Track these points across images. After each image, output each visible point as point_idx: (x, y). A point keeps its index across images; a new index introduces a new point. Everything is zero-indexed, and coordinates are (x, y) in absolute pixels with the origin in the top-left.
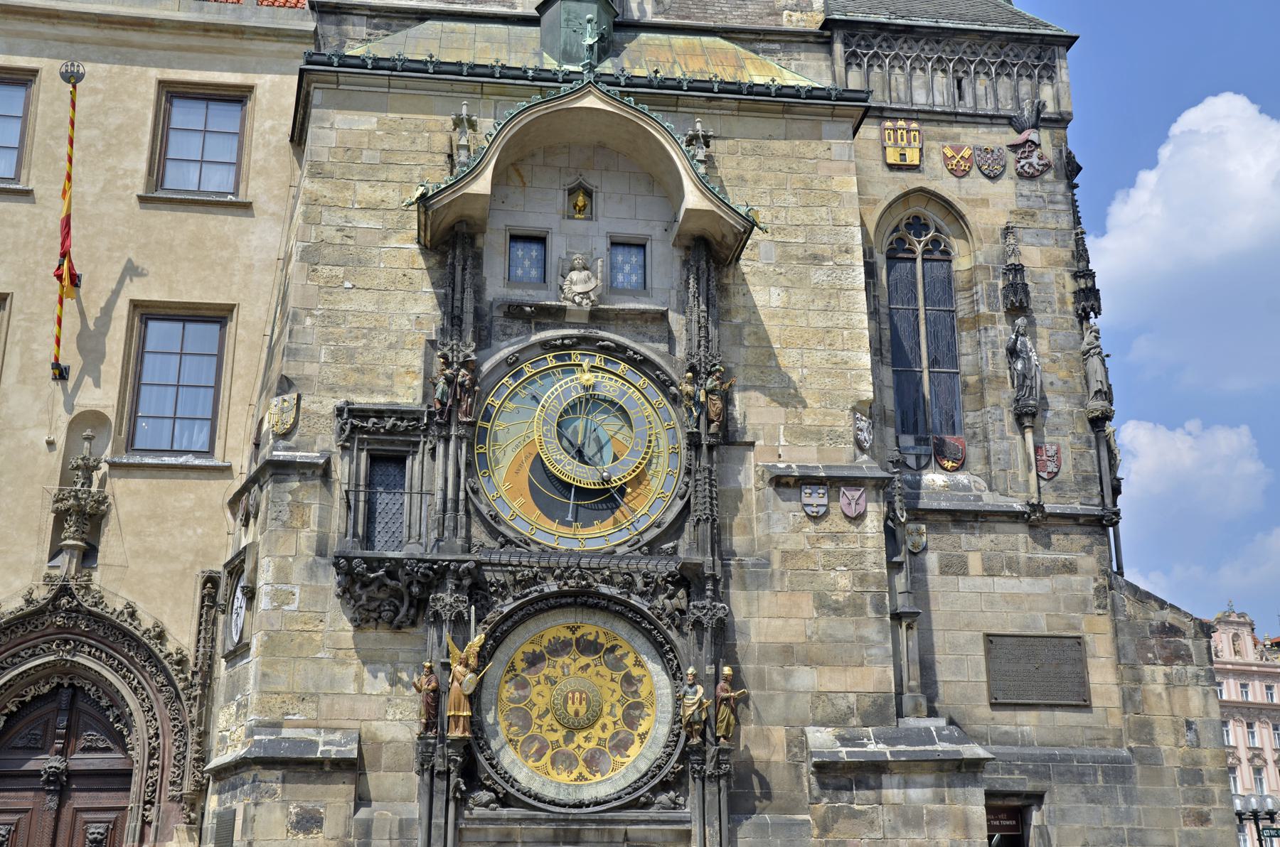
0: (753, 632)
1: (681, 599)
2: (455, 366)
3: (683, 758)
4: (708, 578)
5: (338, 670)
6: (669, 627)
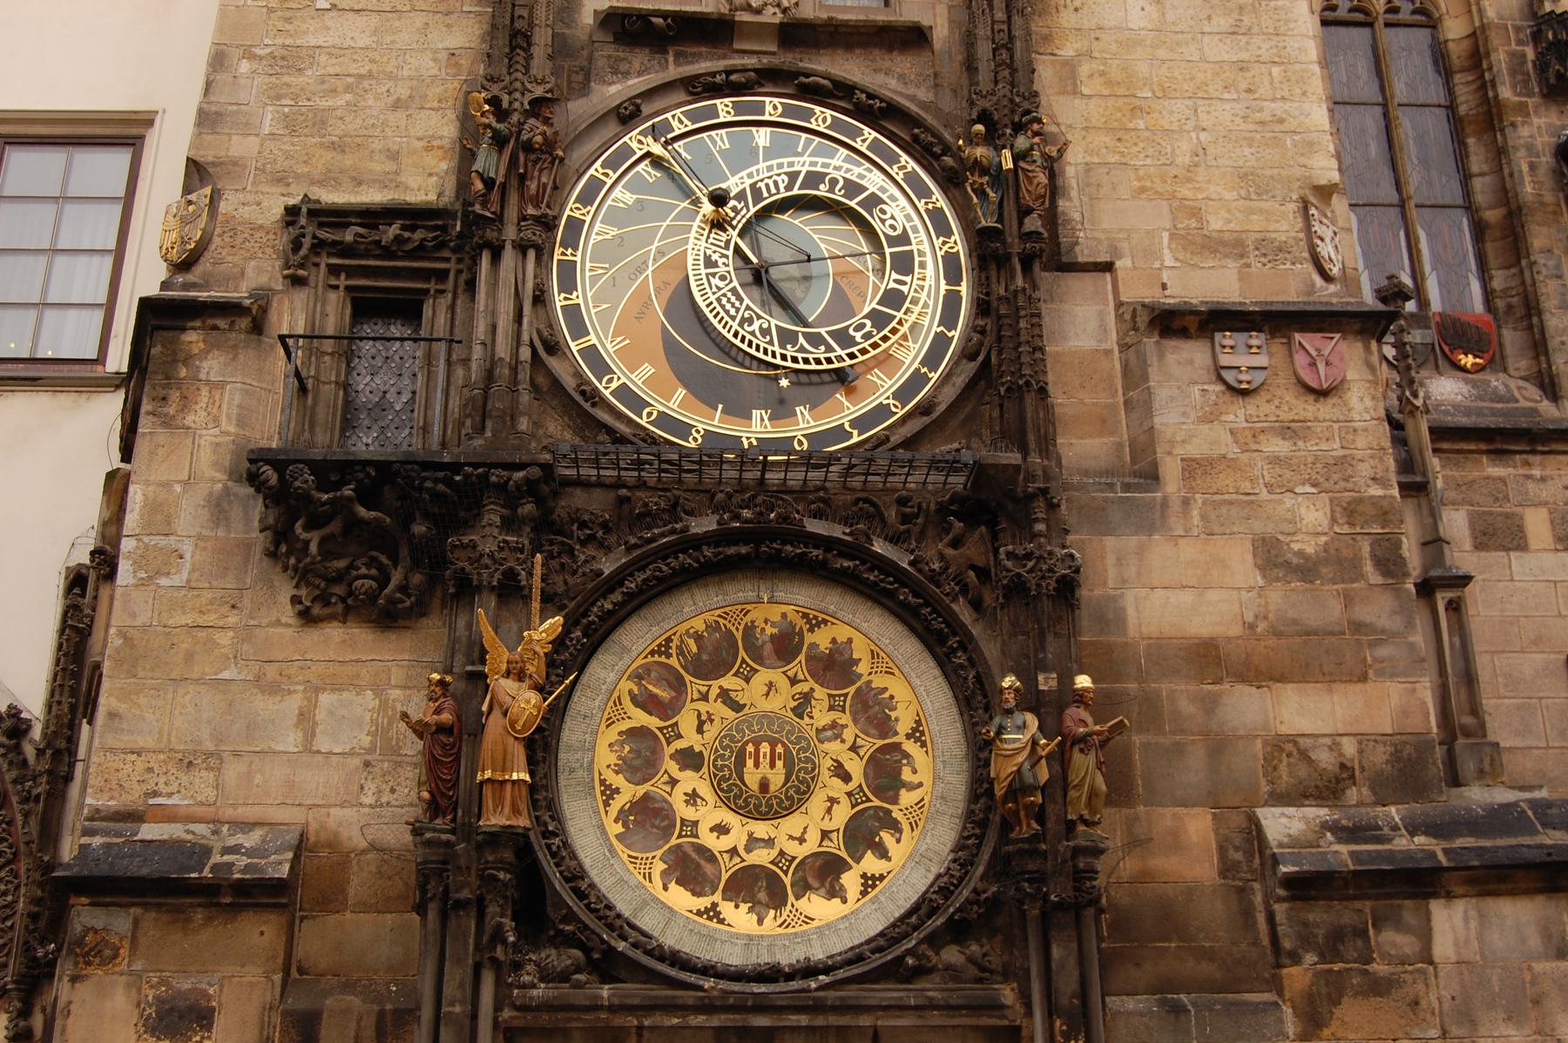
0: (1131, 612)
1: (974, 550)
2: (515, 118)
3: (1001, 867)
4: (1033, 497)
5: (264, 706)
6: (955, 599)
